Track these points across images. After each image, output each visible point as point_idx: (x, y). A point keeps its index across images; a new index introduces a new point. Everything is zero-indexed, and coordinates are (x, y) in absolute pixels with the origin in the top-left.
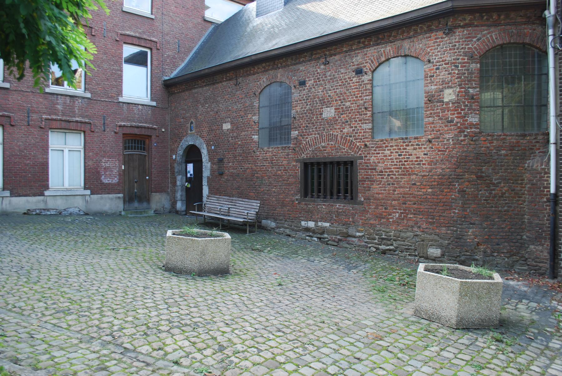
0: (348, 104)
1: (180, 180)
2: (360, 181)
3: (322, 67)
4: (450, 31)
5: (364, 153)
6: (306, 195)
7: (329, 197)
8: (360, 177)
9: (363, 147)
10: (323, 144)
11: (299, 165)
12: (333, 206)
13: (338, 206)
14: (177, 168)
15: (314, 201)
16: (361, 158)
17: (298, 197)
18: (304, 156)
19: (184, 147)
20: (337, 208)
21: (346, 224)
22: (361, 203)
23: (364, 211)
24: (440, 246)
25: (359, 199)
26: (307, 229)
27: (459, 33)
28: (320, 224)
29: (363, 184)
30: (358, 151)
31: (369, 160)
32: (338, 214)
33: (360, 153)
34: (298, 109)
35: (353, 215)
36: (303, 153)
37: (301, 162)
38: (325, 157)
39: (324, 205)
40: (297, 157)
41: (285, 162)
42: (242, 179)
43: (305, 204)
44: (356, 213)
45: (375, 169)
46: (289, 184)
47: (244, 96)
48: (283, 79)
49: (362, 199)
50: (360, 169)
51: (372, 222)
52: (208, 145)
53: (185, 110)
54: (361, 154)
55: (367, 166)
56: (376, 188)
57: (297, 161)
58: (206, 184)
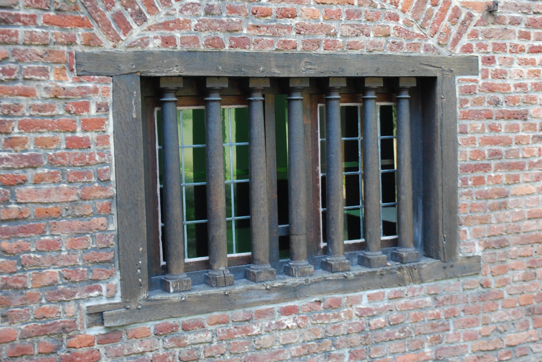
2: (466, 169)
5: (481, 46)
6: (159, 274)
7: (263, 267)
8: (465, 153)
9: (477, 15)
11: (101, 92)
12: (336, 305)
13: (365, 304)
15: (228, 302)
16: (469, 66)
17: (109, 292)
18: (144, 37)
20: (362, 313)
22: (473, 266)
23: (482, 298)
25: (462, 252)
29: (479, 181)
30: (460, 34)
31: (500, 75)
33: (465, 40)
36: (140, 17)
37: (115, 76)
38: (288, 56)
39: (287, 312)
40: (91, 41)
43: (159, 333)
44: (451, 314)
45: (523, 116)
49: (478, 250)
50: (467, 116)
51: (514, 337)
54: (468, 48)
55: (497, 103)
57: (83, 67)
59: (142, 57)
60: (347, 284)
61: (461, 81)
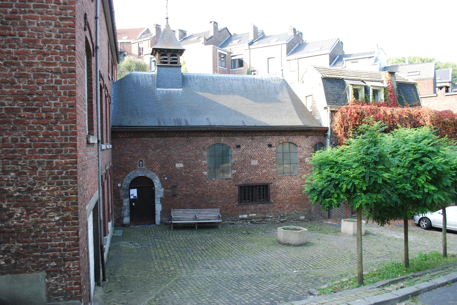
0: (265, 159)
1: (126, 202)
3: (250, 140)
4: (307, 136)
6: (241, 202)
8: (271, 192)
10: (252, 177)
11: (237, 187)
14: (122, 193)
15: (247, 205)
16: (272, 183)
17: (237, 203)
19: (132, 178)
21: (265, 213)
22: (272, 203)
24: (304, 215)
26: (243, 219)
27: (310, 137)
28: (250, 215)
32: (260, 209)
34: (236, 159)
35: (268, 209)
38: (253, 184)
41: (228, 187)
42: (195, 197)
46: (231, 198)
47: (194, 148)
48: (225, 143)
51: (277, 210)
52: (161, 177)
53: (132, 151)
56: (279, 196)
57: (236, 186)
58: (159, 202)
59: (240, 185)
60: (258, 204)
61: (271, 185)
